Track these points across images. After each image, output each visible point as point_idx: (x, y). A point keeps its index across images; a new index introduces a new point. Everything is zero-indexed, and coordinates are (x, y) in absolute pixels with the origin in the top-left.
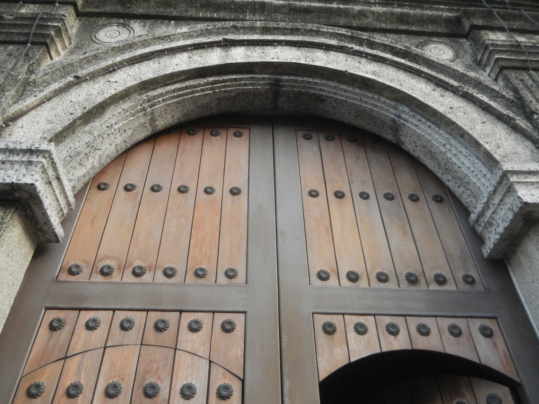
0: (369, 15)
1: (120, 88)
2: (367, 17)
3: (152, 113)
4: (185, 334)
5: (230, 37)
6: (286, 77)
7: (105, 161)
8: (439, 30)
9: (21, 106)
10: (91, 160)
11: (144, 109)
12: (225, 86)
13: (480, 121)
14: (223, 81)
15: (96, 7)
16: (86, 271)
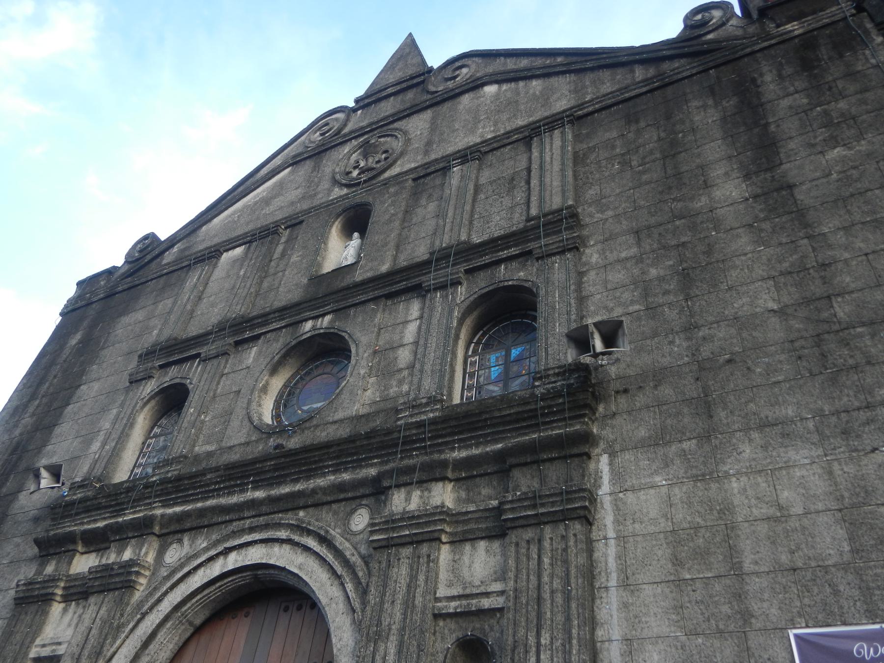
0: (319, 491)
1: (161, 616)
2: (317, 494)
3: (188, 620)
5: (228, 544)
6: (259, 572)
9: (112, 650)
11: (181, 622)
12: (227, 587)
13: (341, 613)
14: (225, 584)
15: (167, 528)
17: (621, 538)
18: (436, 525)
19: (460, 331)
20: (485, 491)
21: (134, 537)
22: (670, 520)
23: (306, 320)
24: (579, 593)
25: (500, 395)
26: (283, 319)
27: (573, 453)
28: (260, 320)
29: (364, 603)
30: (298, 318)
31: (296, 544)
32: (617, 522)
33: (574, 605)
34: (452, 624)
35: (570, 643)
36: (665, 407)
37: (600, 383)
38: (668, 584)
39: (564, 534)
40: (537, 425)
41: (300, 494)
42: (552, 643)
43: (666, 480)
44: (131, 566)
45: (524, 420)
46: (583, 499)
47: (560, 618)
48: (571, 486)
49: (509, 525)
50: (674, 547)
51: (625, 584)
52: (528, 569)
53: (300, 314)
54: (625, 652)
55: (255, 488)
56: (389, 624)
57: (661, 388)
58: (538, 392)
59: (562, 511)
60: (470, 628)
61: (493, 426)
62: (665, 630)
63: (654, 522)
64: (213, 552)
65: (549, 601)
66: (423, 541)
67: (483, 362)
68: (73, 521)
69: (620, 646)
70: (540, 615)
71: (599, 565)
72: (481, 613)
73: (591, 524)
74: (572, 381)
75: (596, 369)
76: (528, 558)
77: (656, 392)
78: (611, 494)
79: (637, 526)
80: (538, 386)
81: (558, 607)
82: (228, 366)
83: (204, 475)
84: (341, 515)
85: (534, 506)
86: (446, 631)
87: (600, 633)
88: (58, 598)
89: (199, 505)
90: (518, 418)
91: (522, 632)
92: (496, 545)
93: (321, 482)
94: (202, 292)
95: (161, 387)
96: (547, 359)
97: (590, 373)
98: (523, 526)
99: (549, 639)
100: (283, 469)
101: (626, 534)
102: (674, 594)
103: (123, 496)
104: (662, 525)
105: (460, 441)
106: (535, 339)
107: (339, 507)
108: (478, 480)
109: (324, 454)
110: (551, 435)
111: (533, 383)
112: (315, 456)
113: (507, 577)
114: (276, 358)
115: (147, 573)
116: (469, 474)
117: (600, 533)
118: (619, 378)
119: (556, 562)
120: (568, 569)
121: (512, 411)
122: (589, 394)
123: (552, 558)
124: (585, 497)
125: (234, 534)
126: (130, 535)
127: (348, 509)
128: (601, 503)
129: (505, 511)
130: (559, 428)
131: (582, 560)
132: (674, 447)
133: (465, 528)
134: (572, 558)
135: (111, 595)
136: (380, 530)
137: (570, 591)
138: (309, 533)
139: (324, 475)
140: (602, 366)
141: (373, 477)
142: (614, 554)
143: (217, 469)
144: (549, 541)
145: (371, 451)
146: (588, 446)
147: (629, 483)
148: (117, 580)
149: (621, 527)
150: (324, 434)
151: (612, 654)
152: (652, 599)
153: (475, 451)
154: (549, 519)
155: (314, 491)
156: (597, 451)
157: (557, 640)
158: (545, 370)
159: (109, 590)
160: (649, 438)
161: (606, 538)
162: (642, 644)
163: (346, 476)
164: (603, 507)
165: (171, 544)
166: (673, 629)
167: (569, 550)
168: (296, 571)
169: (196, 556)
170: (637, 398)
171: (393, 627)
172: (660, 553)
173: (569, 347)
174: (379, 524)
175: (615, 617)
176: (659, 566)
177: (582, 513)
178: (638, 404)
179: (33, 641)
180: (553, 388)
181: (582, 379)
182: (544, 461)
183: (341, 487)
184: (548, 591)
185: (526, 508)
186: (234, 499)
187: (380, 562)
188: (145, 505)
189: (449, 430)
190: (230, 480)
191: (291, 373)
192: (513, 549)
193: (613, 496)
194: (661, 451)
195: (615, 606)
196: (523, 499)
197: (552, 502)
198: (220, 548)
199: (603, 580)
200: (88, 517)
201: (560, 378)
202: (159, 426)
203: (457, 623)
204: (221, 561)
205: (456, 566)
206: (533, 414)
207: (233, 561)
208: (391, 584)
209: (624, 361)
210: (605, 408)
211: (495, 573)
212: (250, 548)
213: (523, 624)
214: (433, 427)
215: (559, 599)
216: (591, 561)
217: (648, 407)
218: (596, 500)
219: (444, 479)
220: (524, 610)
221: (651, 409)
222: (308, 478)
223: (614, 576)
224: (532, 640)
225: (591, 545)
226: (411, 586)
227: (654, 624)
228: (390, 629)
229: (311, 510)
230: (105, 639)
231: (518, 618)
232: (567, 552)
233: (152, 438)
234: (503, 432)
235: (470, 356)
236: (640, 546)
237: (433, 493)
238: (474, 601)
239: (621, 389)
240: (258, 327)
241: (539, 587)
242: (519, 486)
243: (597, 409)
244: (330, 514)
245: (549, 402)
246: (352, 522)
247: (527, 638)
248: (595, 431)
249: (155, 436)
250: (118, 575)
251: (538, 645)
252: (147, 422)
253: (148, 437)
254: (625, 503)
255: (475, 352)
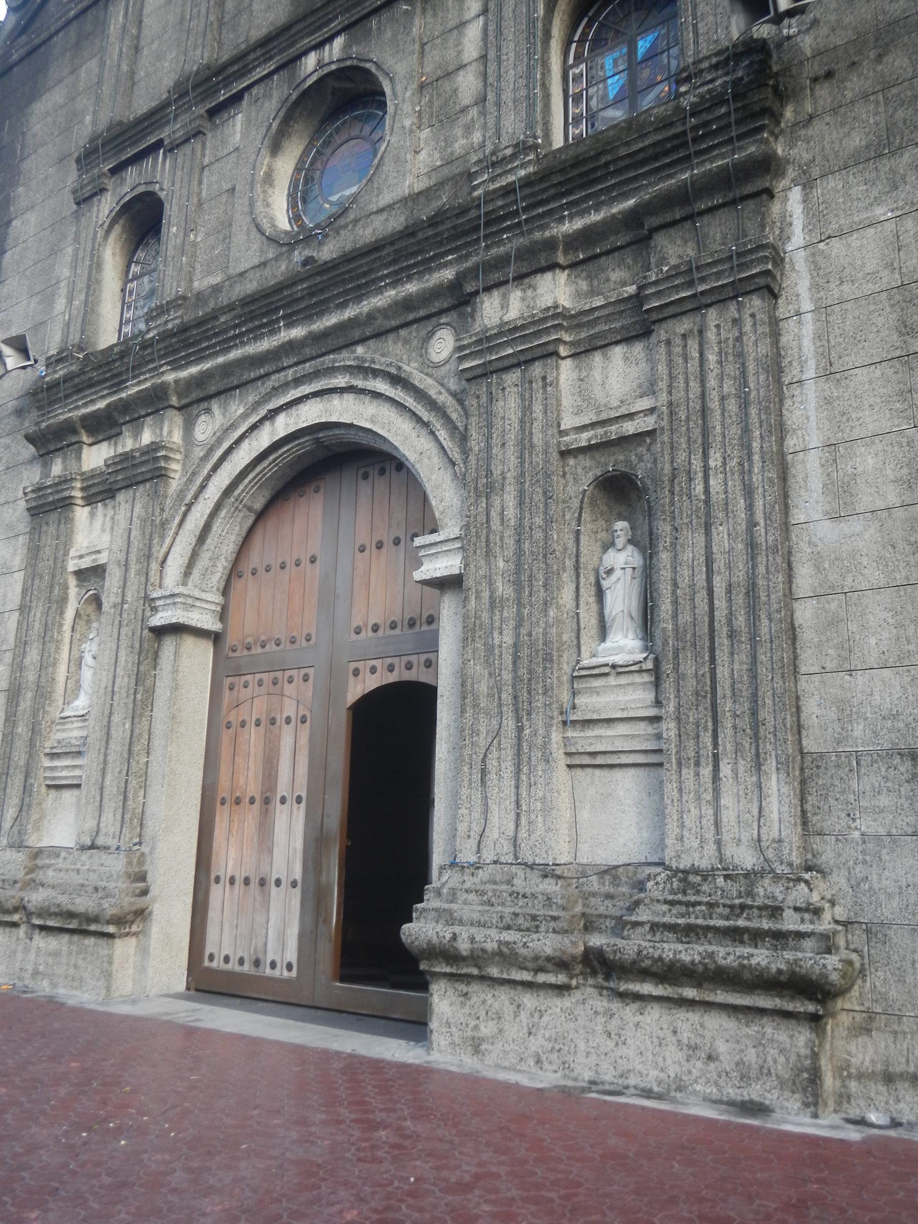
0: (377, 315)
1: (211, 505)
2: (376, 319)
3: (245, 506)
4: (287, 686)
5: (273, 405)
6: (321, 435)
7: (231, 557)
8: (446, 305)
9: (164, 550)
10: (220, 565)
16: (240, 648)
17: (822, 309)
18: (549, 334)
19: (551, 23)
20: (616, 275)
21: (148, 415)
22: (897, 271)
23: (305, 53)
24: (762, 394)
25: (625, 121)
26: (271, 58)
27: (745, 193)
28: (236, 68)
29: (465, 452)
30: (292, 52)
31: (362, 391)
32: (815, 287)
33: (753, 411)
34: (585, 461)
35: (750, 459)
36: (894, 91)
37: (786, 70)
38: (891, 363)
39: (737, 316)
40: (688, 158)
41: (352, 323)
42: (724, 464)
43: (892, 211)
44: (156, 450)
45: (666, 153)
46: (765, 259)
47: (735, 431)
48: (745, 244)
49: (655, 316)
50: (902, 310)
51: (828, 373)
52: (686, 373)
53: (293, 44)
54: (827, 461)
55: (290, 325)
56: (503, 473)
57: (888, 59)
58: (685, 102)
59: (733, 282)
60: (611, 463)
61: (618, 172)
62: (885, 425)
63: (872, 276)
64: (254, 419)
65: (719, 412)
66: (534, 360)
67: (594, 71)
68: (66, 405)
69: (821, 454)
70: (706, 432)
71: (790, 352)
72: (624, 441)
73: (775, 296)
74: (740, 74)
75: (779, 45)
76: (686, 358)
77: (879, 68)
78: (805, 247)
79: (846, 288)
80: (686, 93)
81: (731, 417)
82: (207, 152)
83: (215, 318)
84: (415, 343)
85: (690, 284)
86: (579, 471)
87: (791, 443)
88: (79, 502)
89: (221, 360)
90: (658, 152)
91: (682, 457)
92: (638, 348)
93: (378, 301)
94: (138, 37)
95: (122, 203)
96: (696, 42)
97: (769, 55)
98: (674, 316)
99: (720, 460)
100: (322, 291)
101: (830, 302)
102: (900, 375)
103: (117, 364)
104: (885, 280)
105: (570, 204)
106: (675, 15)
107: (410, 333)
108: (603, 259)
109: (374, 260)
110: (711, 170)
111: (677, 90)
112: (361, 266)
113: (656, 388)
114: (275, 126)
115: (178, 457)
116: (589, 253)
117: (791, 307)
118: (818, 53)
119: (726, 358)
120: (743, 364)
121: (647, 143)
122: (769, 89)
123: (720, 353)
124: (766, 257)
125: (276, 391)
126: (143, 413)
127: (423, 333)
128: (792, 263)
129: (648, 298)
130: (722, 156)
131: (764, 348)
132: (906, 156)
133: (592, 332)
134: (749, 348)
135: (141, 488)
136: (471, 354)
137: (749, 393)
138: (376, 373)
139: (380, 291)
140: (789, 38)
141: (450, 281)
142: (811, 333)
143: (231, 307)
144: (714, 330)
145: (441, 244)
146: (769, 178)
147: (834, 226)
148: (143, 469)
149: (822, 293)
150: (369, 231)
151: (808, 466)
152: (867, 386)
153: (595, 217)
154: (713, 299)
155: (371, 316)
156: (784, 183)
157: (732, 459)
158: (694, 63)
159: (138, 483)
160: (867, 147)
161: (798, 314)
162: (851, 448)
163: (412, 288)
164: (793, 269)
165: (198, 416)
166: (896, 422)
167: (745, 338)
168: (368, 425)
169: (233, 426)
170: (848, 84)
171: (508, 475)
172: (880, 321)
173: (733, 12)
174: (469, 345)
175: (813, 418)
176: (878, 339)
177: (762, 281)
178: (849, 95)
179: (66, 554)
180: (709, 92)
181: (756, 66)
182: (701, 213)
183: (407, 304)
184: (717, 399)
185: (677, 288)
186: (265, 345)
187: (478, 397)
188: (150, 371)
189: (552, 191)
190: (252, 319)
191: (301, 148)
192: (662, 349)
193: (810, 250)
194: (885, 165)
195: (812, 405)
196: (672, 276)
197: (716, 273)
198: (262, 412)
199: (795, 372)
200: (82, 398)
201: (720, 72)
202: (137, 263)
203: (593, 458)
204: (267, 427)
205: (584, 386)
206: (680, 142)
207: (283, 425)
208: (498, 423)
209: (826, 23)
210: (795, 111)
211: (640, 386)
212: (301, 406)
213: (684, 446)
214: (527, 191)
215: (732, 406)
216: (778, 348)
217: (865, 96)
218: (783, 260)
219: (552, 267)
220: (684, 429)
221: (872, 98)
222: (359, 299)
223: (812, 364)
224: (697, 464)
225: (777, 324)
226: (525, 422)
227: (869, 420)
228: (504, 479)
229: (371, 343)
230: (151, 539)
231: (675, 439)
232: (742, 342)
233: (132, 281)
234: (635, 178)
235: (572, 66)
236: (850, 316)
237: (539, 291)
238: (613, 428)
239: (822, 72)
240: (236, 80)
241: (703, 396)
242: (665, 258)
243: (781, 115)
244: (400, 344)
245: (706, 117)
246: (430, 350)
247: (690, 463)
248: (780, 151)
249: (136, 278)
250: (143, 463)
251: (706, 469)
252: (118, 258)
253: (126, 281)
254: (827, 257)
255: (578, 58)
